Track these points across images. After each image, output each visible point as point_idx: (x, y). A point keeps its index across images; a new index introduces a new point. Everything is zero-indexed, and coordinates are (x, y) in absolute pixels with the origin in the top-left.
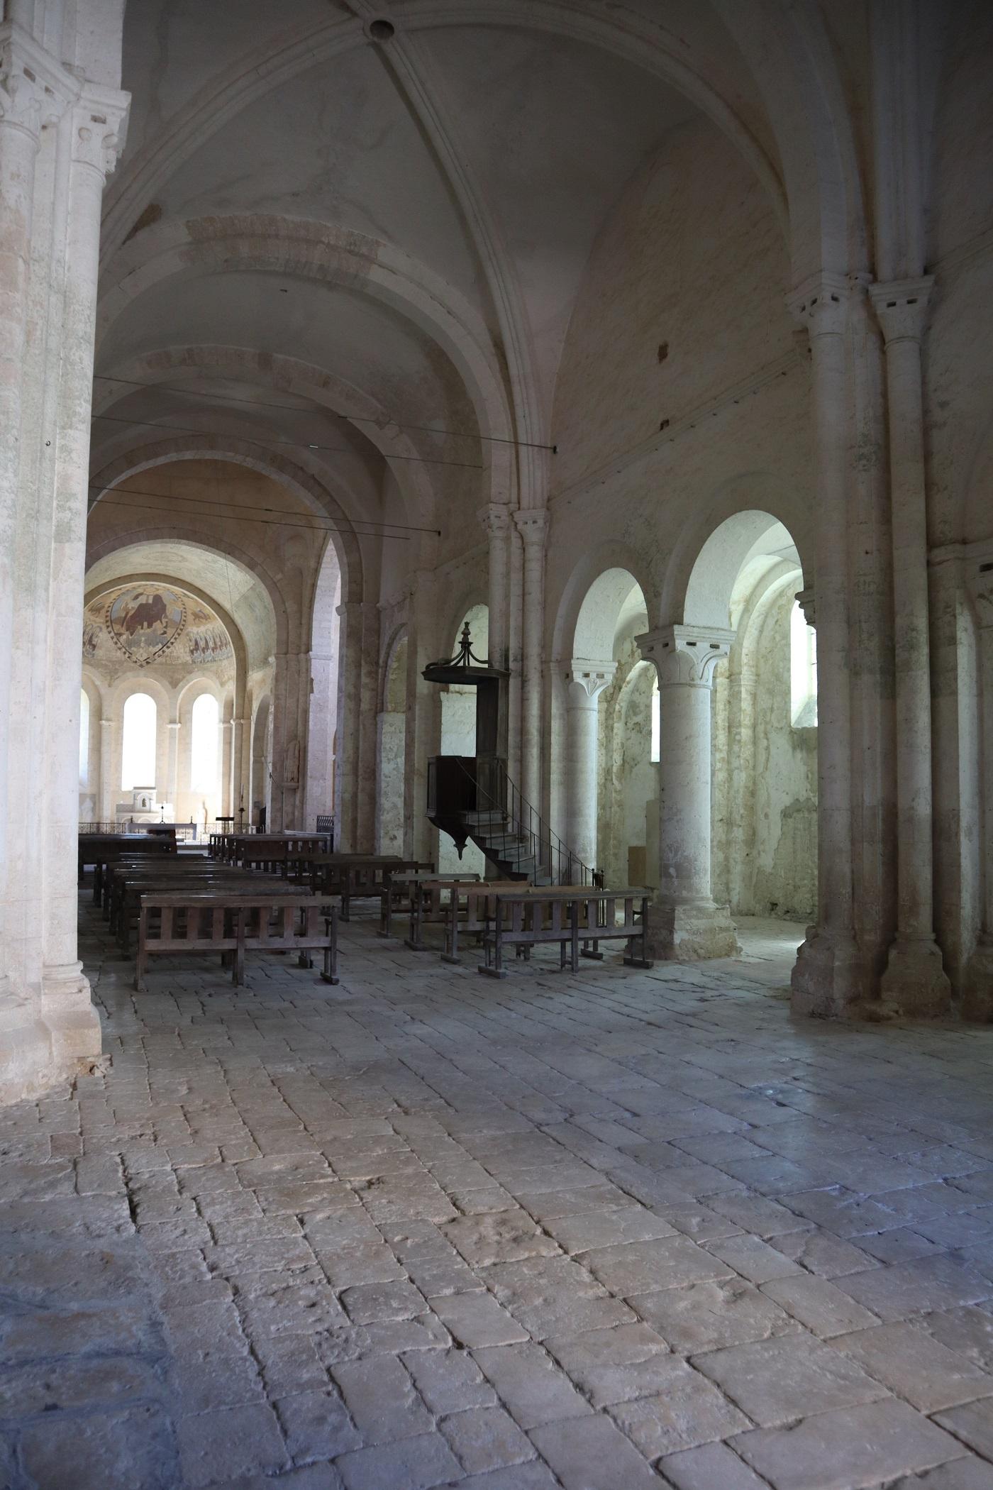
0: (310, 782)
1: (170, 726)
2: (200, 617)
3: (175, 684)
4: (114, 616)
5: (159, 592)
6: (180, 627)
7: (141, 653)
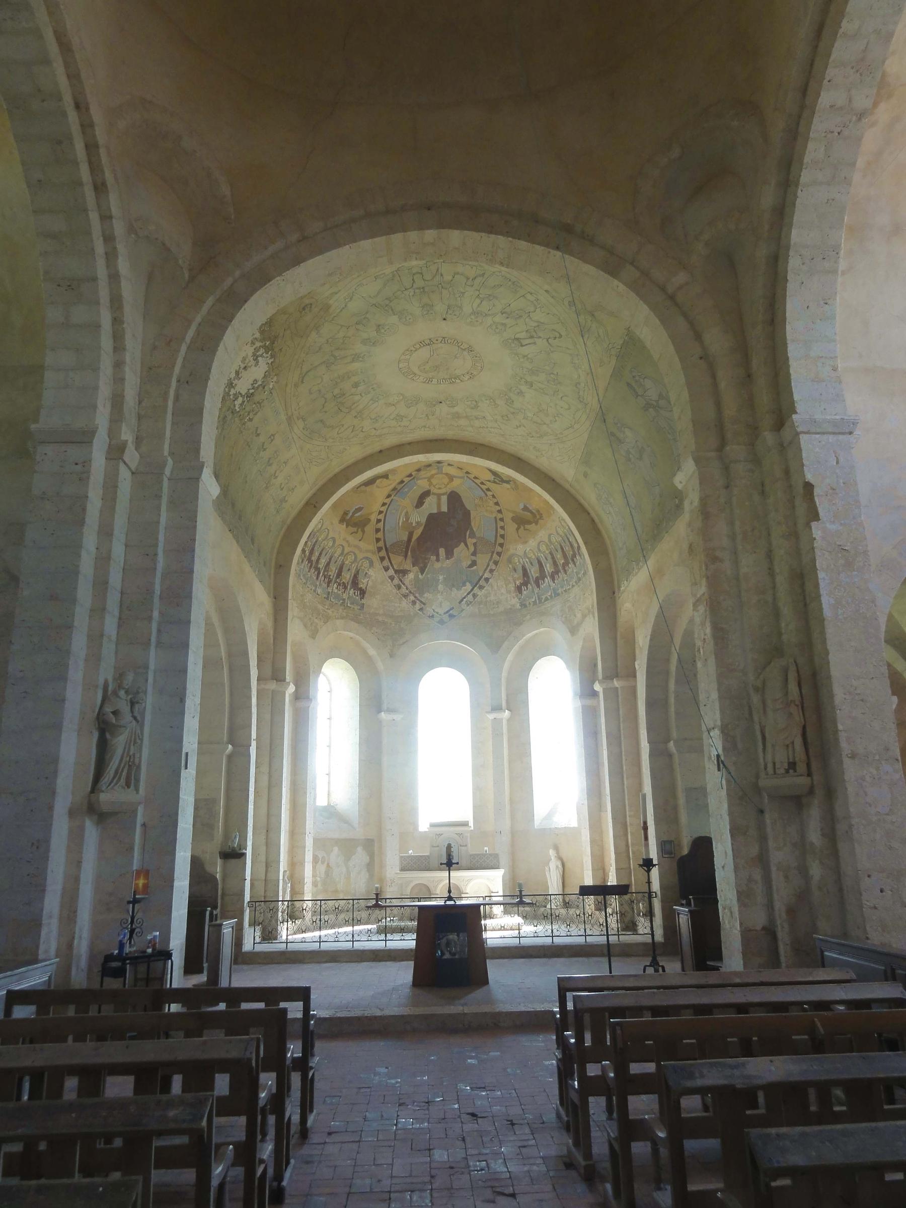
0: (851, 771)
1: (491, 716)
2: (528, 519)
3: (496, 646)
4: (391, 539)
5: (456, 485)
6: (496, 547)
7: (440, 601)
